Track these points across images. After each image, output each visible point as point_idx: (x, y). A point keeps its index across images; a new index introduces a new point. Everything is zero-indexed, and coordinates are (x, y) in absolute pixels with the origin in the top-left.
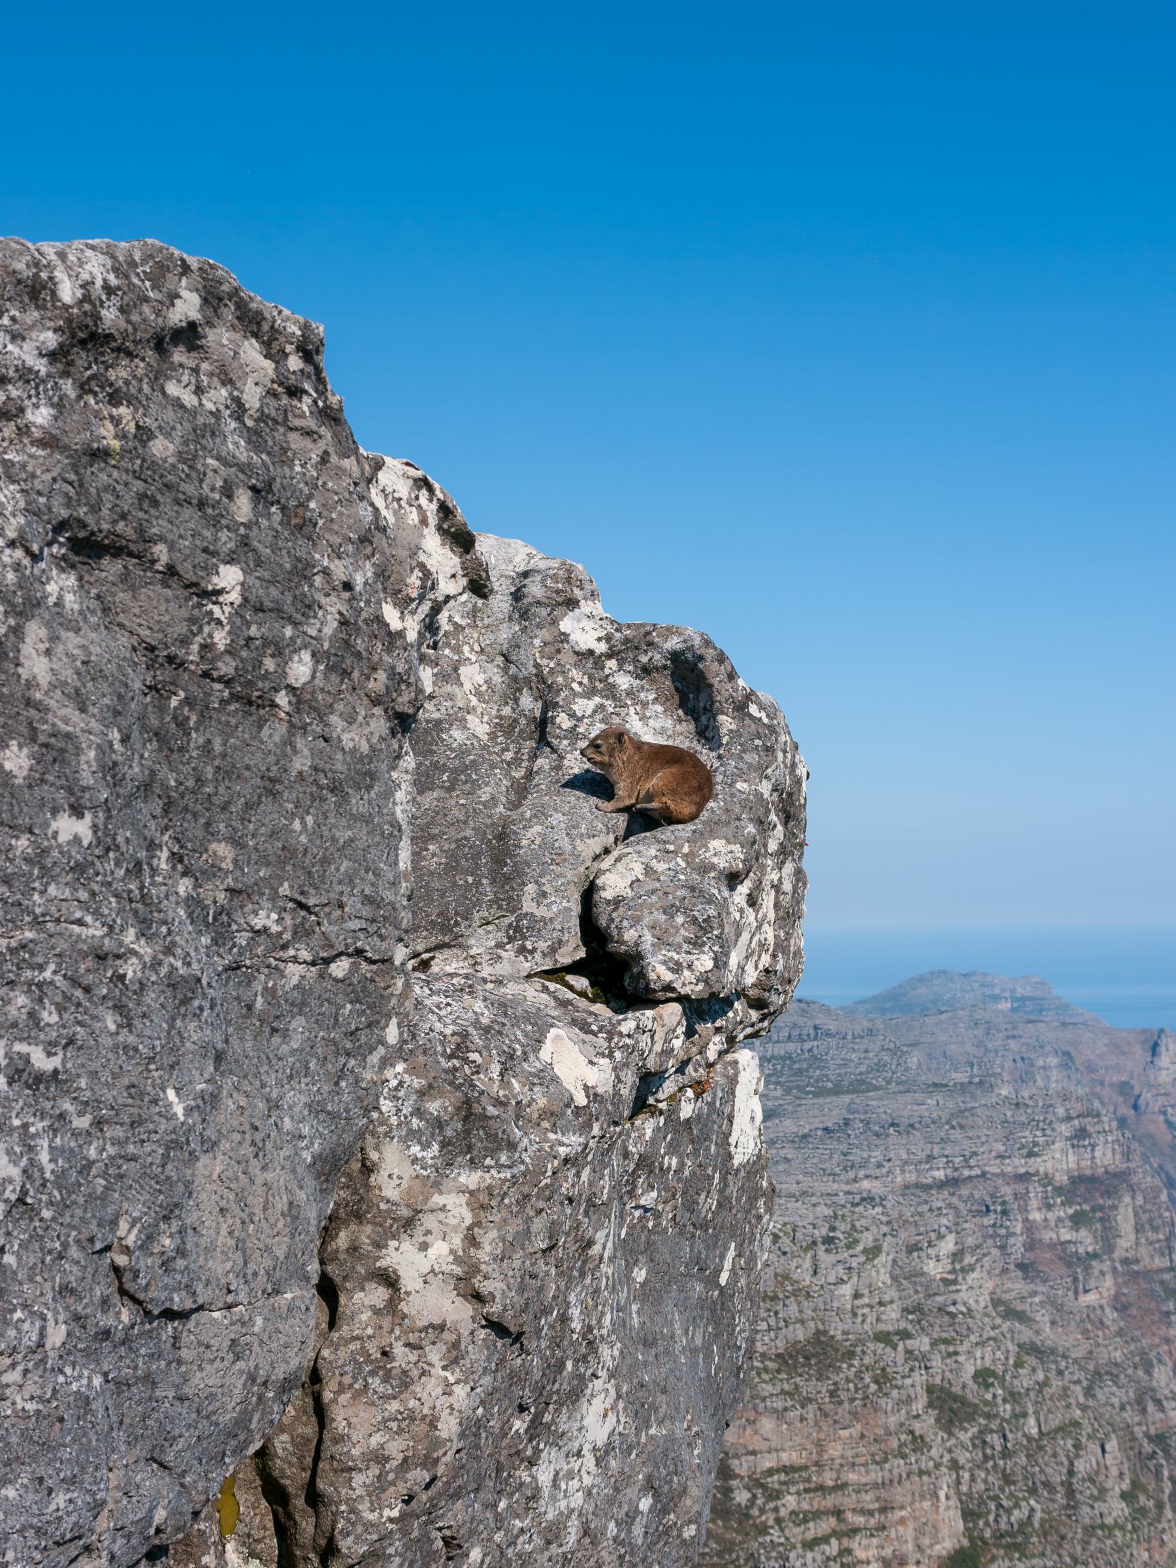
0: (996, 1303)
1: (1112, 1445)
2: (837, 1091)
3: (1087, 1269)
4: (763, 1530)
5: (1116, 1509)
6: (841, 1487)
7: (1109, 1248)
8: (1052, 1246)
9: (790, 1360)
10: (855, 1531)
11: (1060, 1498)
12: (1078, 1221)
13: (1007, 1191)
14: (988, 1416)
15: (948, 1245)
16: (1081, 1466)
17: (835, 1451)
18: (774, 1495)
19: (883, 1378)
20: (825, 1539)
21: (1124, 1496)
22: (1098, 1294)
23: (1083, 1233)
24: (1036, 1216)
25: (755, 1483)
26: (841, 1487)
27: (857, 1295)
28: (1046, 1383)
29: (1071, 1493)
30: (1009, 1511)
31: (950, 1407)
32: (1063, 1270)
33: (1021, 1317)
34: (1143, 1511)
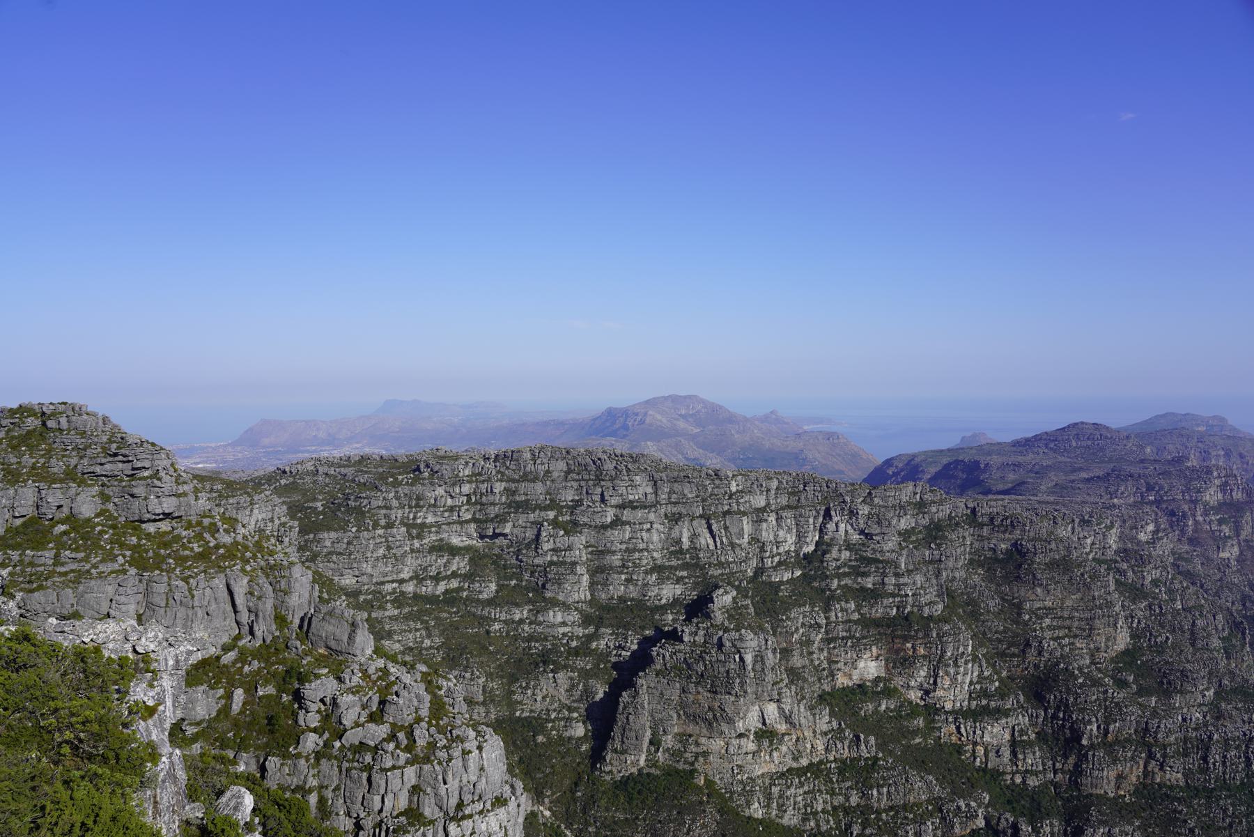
0: (1173, 553)
1: (1220, 617)
2: (1110, 461)
3: (1224, 545)
4: (1035, 630)
5: (1216, 643)
6: (1071, 618)
7: (1238, 536)
8: (1207, 532)
9: (1052, 565)
10: (1075, 636)
11: (1187, 635)
12: (1220, 522)
13: (1186, 507)
14: (1154, 598)
15: (1151, 527)
16: (1200, 623)
17: (1068, 603)
18: (1042, 618)
19: (1094, 577)
20: (1063, 638)
21: (1223, 639)
22: (1230, 553)
23: (1224, 527)
24: (1201, 519)
25: (1032, 612)
26: (1071, 618)
27: (1093, 544)
28: (1187, 587)
29: (1192, 633)
30: (1156, 637)
31: (1135, 592)
32: (1211, 542)
33: (1186, 560)
34: (1234, 646)
